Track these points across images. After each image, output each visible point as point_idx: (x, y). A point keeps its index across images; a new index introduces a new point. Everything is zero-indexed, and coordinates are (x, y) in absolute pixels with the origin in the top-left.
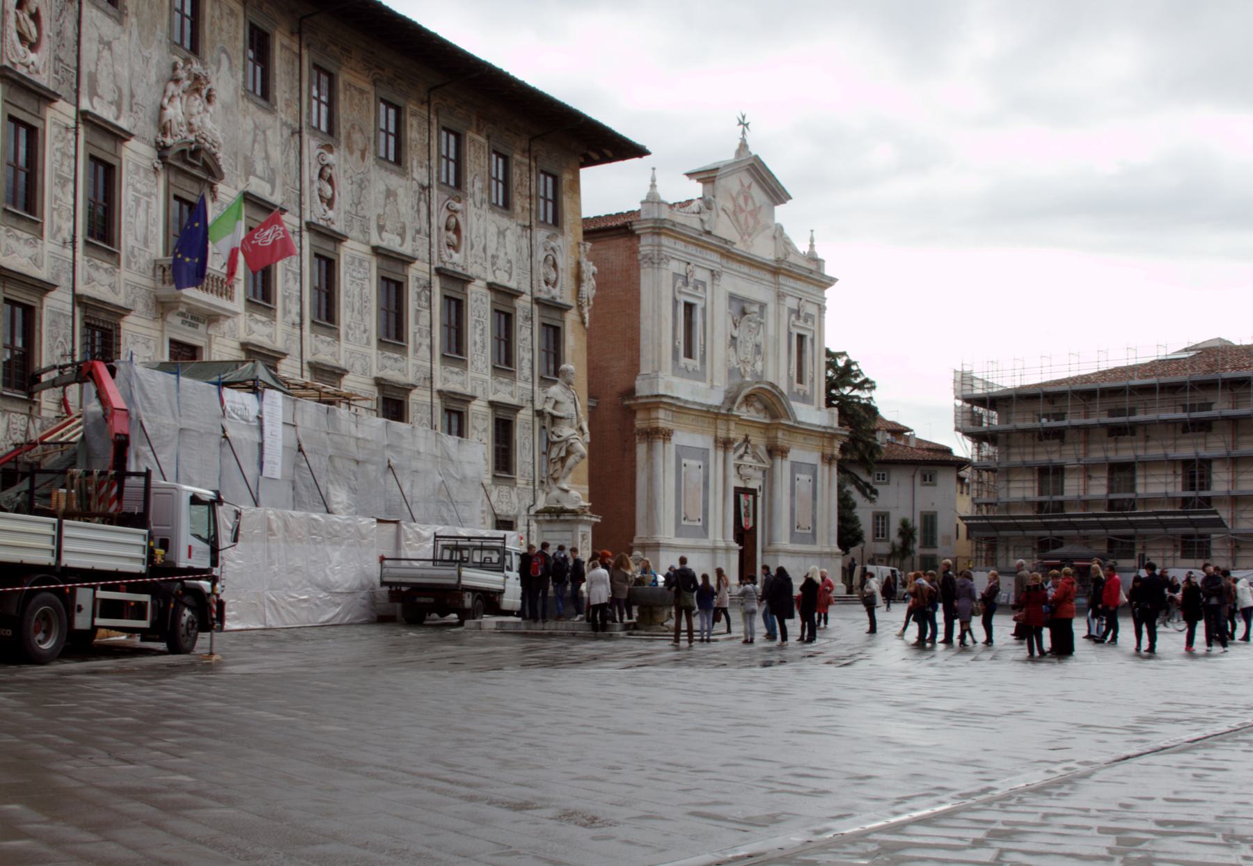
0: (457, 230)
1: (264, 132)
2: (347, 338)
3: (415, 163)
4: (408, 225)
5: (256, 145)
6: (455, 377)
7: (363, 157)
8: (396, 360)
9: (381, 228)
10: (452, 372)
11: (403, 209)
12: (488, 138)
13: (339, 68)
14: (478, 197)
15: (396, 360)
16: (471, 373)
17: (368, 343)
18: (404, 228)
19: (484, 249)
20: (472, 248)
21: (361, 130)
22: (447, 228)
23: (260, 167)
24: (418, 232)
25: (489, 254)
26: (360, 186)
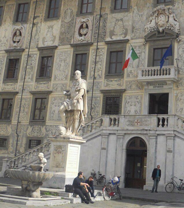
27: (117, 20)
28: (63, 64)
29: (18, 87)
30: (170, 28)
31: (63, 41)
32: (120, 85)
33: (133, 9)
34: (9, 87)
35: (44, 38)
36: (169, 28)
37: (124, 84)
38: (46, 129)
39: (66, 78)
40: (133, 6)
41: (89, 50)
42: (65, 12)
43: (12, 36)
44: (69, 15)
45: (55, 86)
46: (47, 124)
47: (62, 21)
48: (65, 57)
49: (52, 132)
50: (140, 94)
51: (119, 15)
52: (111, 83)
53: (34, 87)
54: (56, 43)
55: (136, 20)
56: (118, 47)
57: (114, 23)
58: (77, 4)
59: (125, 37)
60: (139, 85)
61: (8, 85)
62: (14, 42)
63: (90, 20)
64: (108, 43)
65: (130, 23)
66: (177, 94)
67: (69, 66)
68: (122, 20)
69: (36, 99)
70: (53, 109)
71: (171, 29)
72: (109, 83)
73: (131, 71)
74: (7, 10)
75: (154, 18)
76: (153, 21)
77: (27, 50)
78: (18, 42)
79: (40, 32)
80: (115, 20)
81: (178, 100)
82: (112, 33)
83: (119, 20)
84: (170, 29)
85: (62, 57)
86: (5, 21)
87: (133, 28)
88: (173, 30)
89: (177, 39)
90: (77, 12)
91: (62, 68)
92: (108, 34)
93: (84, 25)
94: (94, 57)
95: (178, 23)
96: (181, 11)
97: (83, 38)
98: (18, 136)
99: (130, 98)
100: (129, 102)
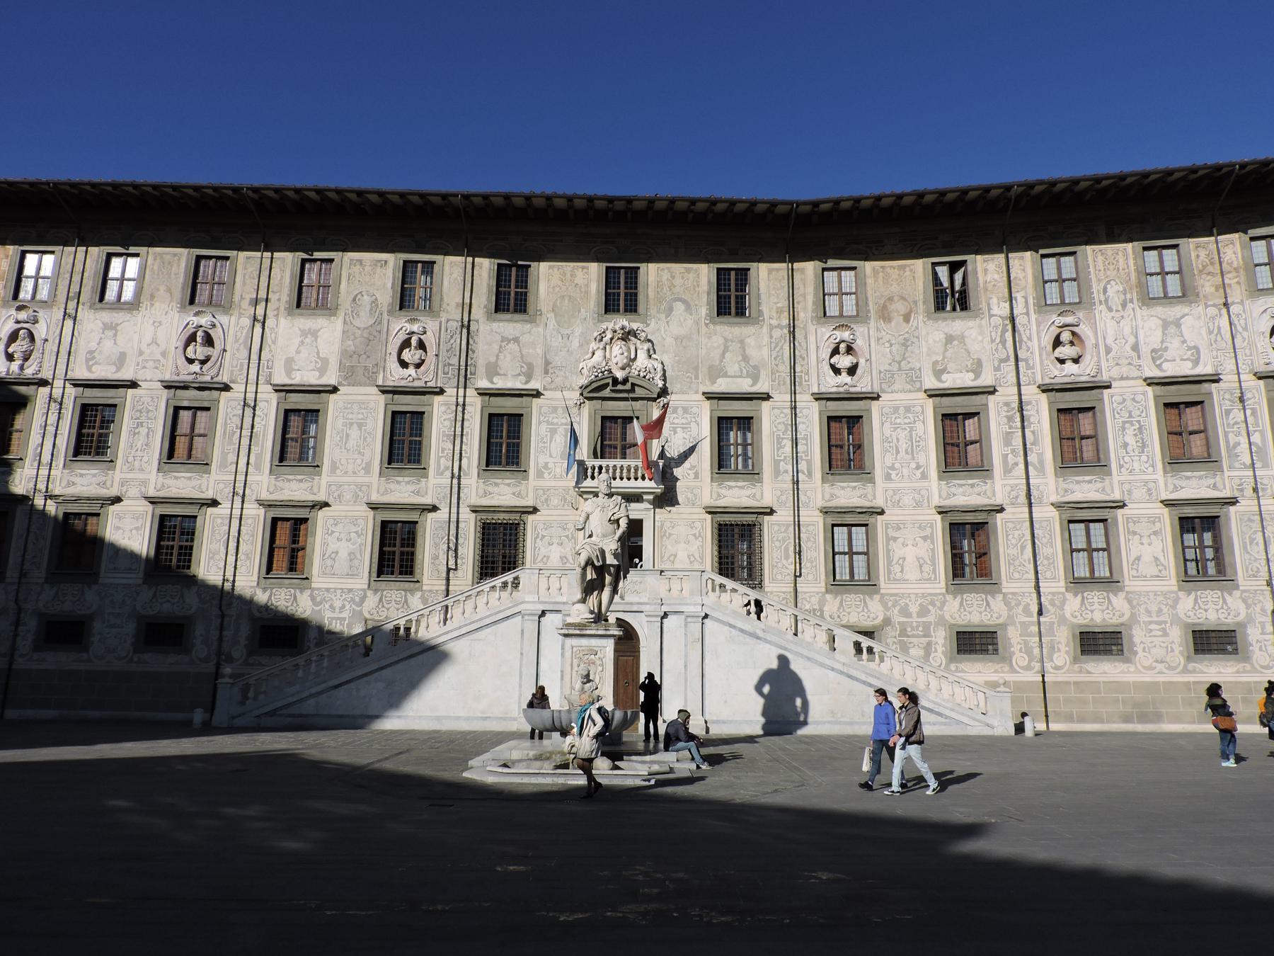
1: (742, 342)
2: (888, 477)
4: (984, 359)
6: (1085, 486)
9: (938, 374)
10: (1078, 482)
11: (974, 347)
14: (1115, 301)
15: (972, 486)
17: (924, 476)
19: (1135, 348)
21: (903, 298)
23: (733, 368)
25: (1145, 350)
26: (904, 345)
27: (504, 339)
28: (354, 433)
29: (211, 484)
31: (350, 374)
32: (519, 495)
33: (544, 318)
34: (180, 483)
35: (289, 362)
37: (531, 494)
38: (313, 598)
39: (367, 469)
40: (544, 310)
41: (431, 405)
42: (354, 300)
43: (181, 344)
44: (368, 308)
45: (334, 488)
46: (313, 585)
47: (345, 322)
48: (360, 416)
49: (331, 606)
50: (572, 518)
51: (509, 326)
52: (496, 489)
53: (265, 486)
54: (330, 379)
55: (555, 344)
56: (508, 406)
57: (496, 347)
58: (389, 285)
59: (527, 383)
60: (569, 498)
61: (176, 478)
62: (191, 361)
63: (429, 327)
64: (483, 393)
65: (540, 351)
67: (374, 439)
68: (516, 340)
69: (275, 521)
70: (333, 547)
72: (490, 489)
73: (547, 464)
74: (156, 267)
75: (601, 345)
76: (599, 354)
77: (238, 388)
78: (203, 362)
79: (274, 342)
80: (499, 338)
82: (492, 371)
83: (509, 341)
85: (350, 416)
86: (152, 297)
87: (547, 363)
90: (392, 305)
91: (351, 443)
92: (481, 370)
93: (414, 341)
94: (447, 423)
97: (411, 371)
98: (223, 616)
99: (548, 526)
100: (543, 536)
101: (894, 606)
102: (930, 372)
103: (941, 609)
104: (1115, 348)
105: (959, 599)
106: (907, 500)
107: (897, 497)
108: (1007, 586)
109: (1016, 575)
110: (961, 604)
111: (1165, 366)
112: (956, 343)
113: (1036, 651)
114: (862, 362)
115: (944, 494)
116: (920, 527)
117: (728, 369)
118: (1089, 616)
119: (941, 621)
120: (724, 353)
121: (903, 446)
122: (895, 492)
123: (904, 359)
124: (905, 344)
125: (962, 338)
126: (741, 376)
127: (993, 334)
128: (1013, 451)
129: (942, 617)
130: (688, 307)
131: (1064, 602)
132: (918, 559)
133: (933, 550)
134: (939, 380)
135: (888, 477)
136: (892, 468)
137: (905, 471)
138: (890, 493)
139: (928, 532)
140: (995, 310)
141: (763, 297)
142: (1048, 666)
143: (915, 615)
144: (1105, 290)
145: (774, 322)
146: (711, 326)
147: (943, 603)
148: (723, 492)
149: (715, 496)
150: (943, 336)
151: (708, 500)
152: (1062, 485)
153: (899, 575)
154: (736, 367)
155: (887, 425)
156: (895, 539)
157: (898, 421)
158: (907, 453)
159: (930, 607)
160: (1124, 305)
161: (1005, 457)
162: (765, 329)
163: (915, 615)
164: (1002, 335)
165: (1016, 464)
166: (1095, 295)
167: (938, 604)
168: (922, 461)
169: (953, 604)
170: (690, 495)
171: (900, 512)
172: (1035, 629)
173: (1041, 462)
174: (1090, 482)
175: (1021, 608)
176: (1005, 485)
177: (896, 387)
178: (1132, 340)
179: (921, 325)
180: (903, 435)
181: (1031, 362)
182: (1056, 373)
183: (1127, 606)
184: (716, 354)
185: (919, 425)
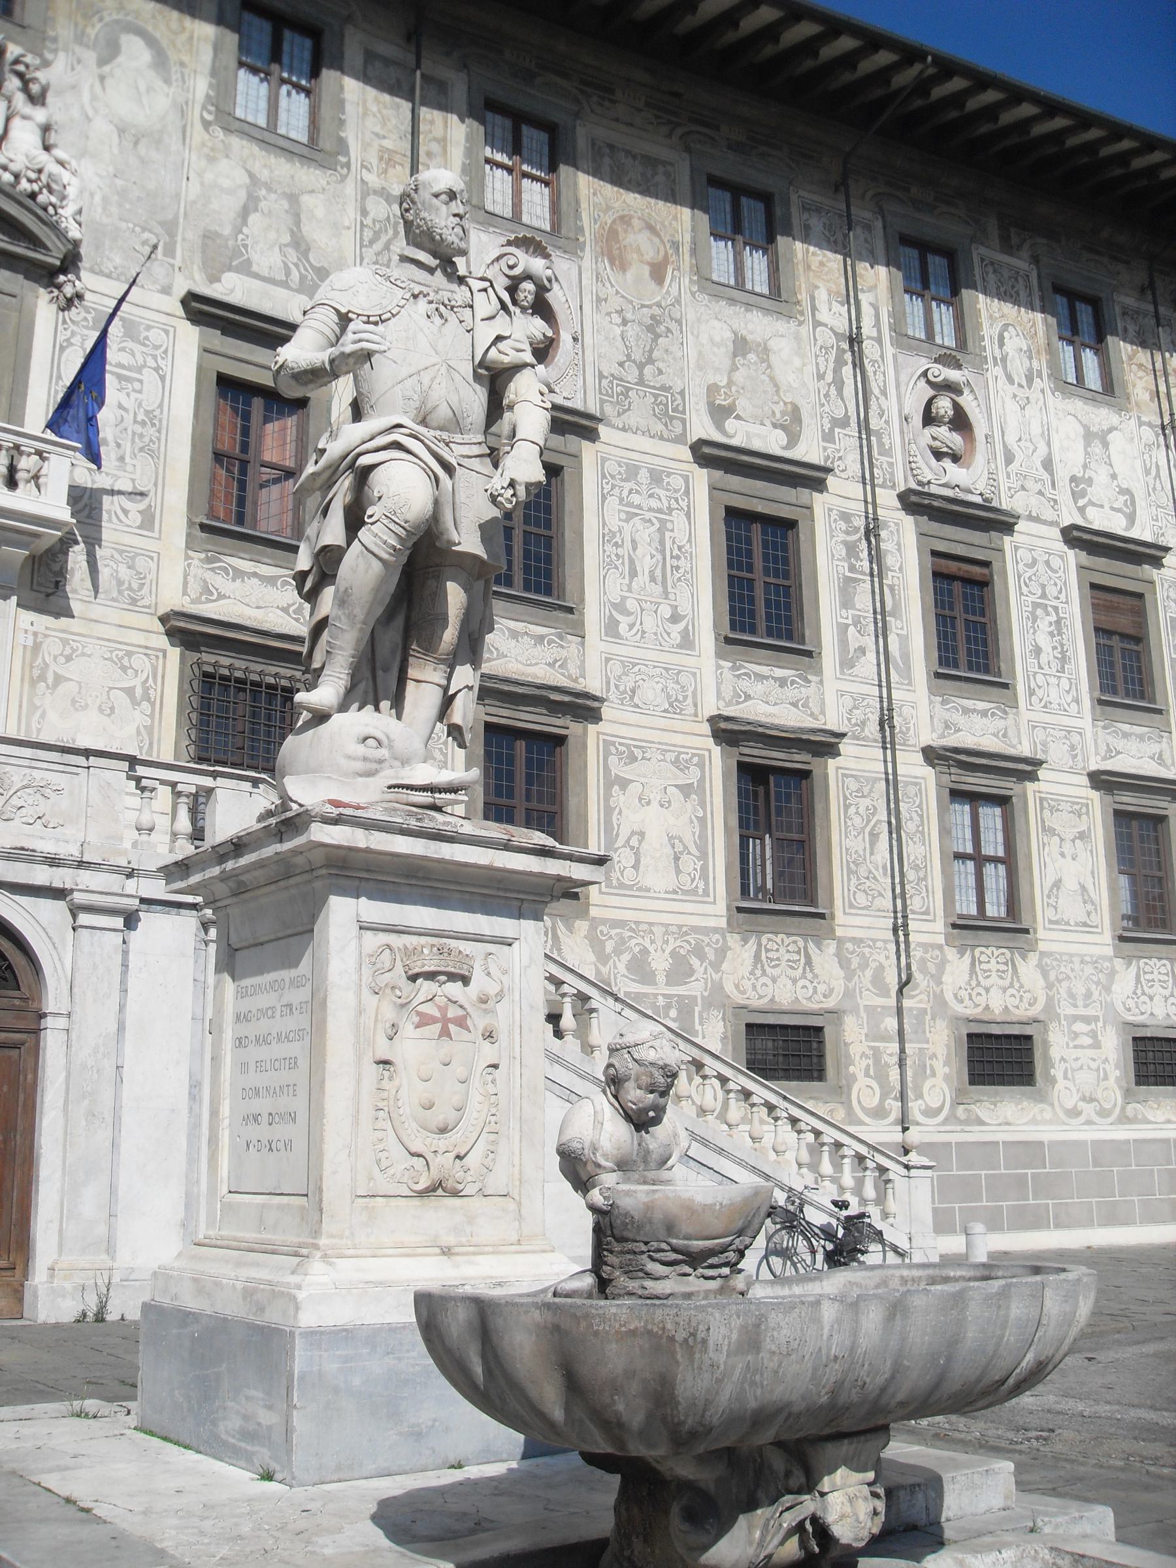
0: (960, 422)
1: (293, 199)
2: (611, 629)
3: (822, 295)
5: (253, 218)
6: (978, 722)
7: (658, 273)
8: (782, 682)
9: (720, 413)
10: (966, 711)
11: (787, 377)
12: (1035, 260)
13: (577, 115)
14: (1019, 366)
15: (782, 682)
16: (1027, 712)
17: (687, 642)
18: (795, 414)
19: (1048, 464)
20: (1009, 459)
21: (651, 228)
22: (929, 418)
23: (266, 259)
24: (844, 423)
25: (1062, 475)
26: (650, 329)
30: (36, 187)
36: (24, 185)
66: (35, 634)
71: (41, 199)
81: (42, 678)
84: (33, 196)
88: (51, 210)
89: (62, 278)
95: (75, 181)
96: (89, 120)
101: (618, 952)
102: (703, 407)
103: (716, 966)
104: (1019, 457)
105: (752, 944)
106: (651, 692)
107: (628, 682)
108: (846, 922)
109: (862, 899)
110: (757, 957)
111: (1091, 512)
112: (752, 357)
113: (894, 1074)
114: (565, 337)
115: (728, 694)
116: (676, 762)
117: (255, 257)
118: (981, 1000)
119: (716, 998)
120: (244, 214)
121: (646, 562)
122: (629, 665)
123: (650, 361)
124: (653, 328)
125: (765, 352)
126: (284, 284)
127: (821, 360)
128: (856, 622)
129: (718, 987)
130: (161, 62)
131: (942, 965)
132: (670, 838)
133: (702, 821)
134: (720, 427)
135: (611, 629)
136: (620, 607)
137: (649, 623)
138: (616, 668)
139: (693, 775)
140: (824, 315)
141: (348, 107)
142: (915, 1107)
143: (661, 978)
144: (1001, 344)
145: (372, 179)
146: (219, 133)
147: (722, 953)
148: (219, 582)
149: (194, 588)
150: (729, 335)
151: (173, 598)
152: (941, 712)
153: (630, 872)
154: (276, 258)
155: (613, 502)
156: (624, 784)
157: (636, 499)
158: (653, 579)
159: (695, 962)
160: (1030, 380)
161: (843, 629)
162: (350, 189)
163: (661, 978)
164: (837, 371)
165: (862, 651)
166: (987, 343)
167: (710, 954)
168: (684, 609)
169: (741, 954)
170: (124, 572)
171: (633, 718)
172: (891, 1023)
173: (906, 656)
174: (984, 713)
175: (869, 973)
176: (841, 693)
177: (632, 419)
178: (1042, 450)
179: (686, 297)
180: (646, 534)
181: (886, 440)
182: (927, 476)
183: (1041, 983)
184: (227, 206)
185: (679, 519)
